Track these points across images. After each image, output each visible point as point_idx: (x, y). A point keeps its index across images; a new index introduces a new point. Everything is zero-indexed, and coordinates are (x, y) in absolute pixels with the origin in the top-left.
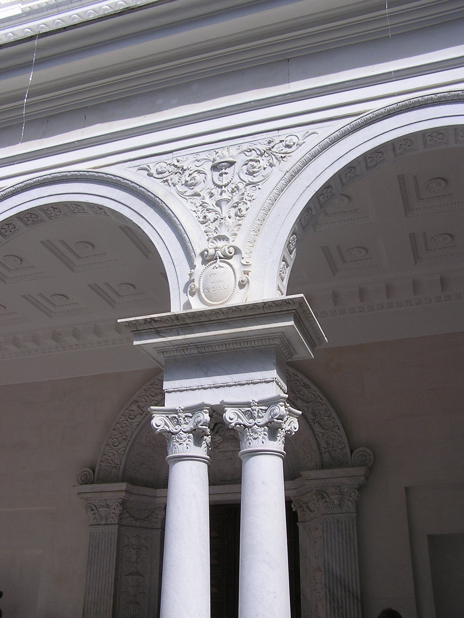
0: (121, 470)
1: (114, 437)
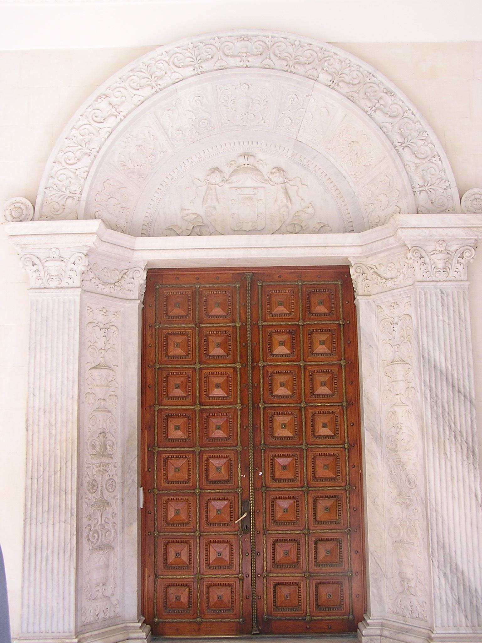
0: (83, 203)
1: (69, 149)
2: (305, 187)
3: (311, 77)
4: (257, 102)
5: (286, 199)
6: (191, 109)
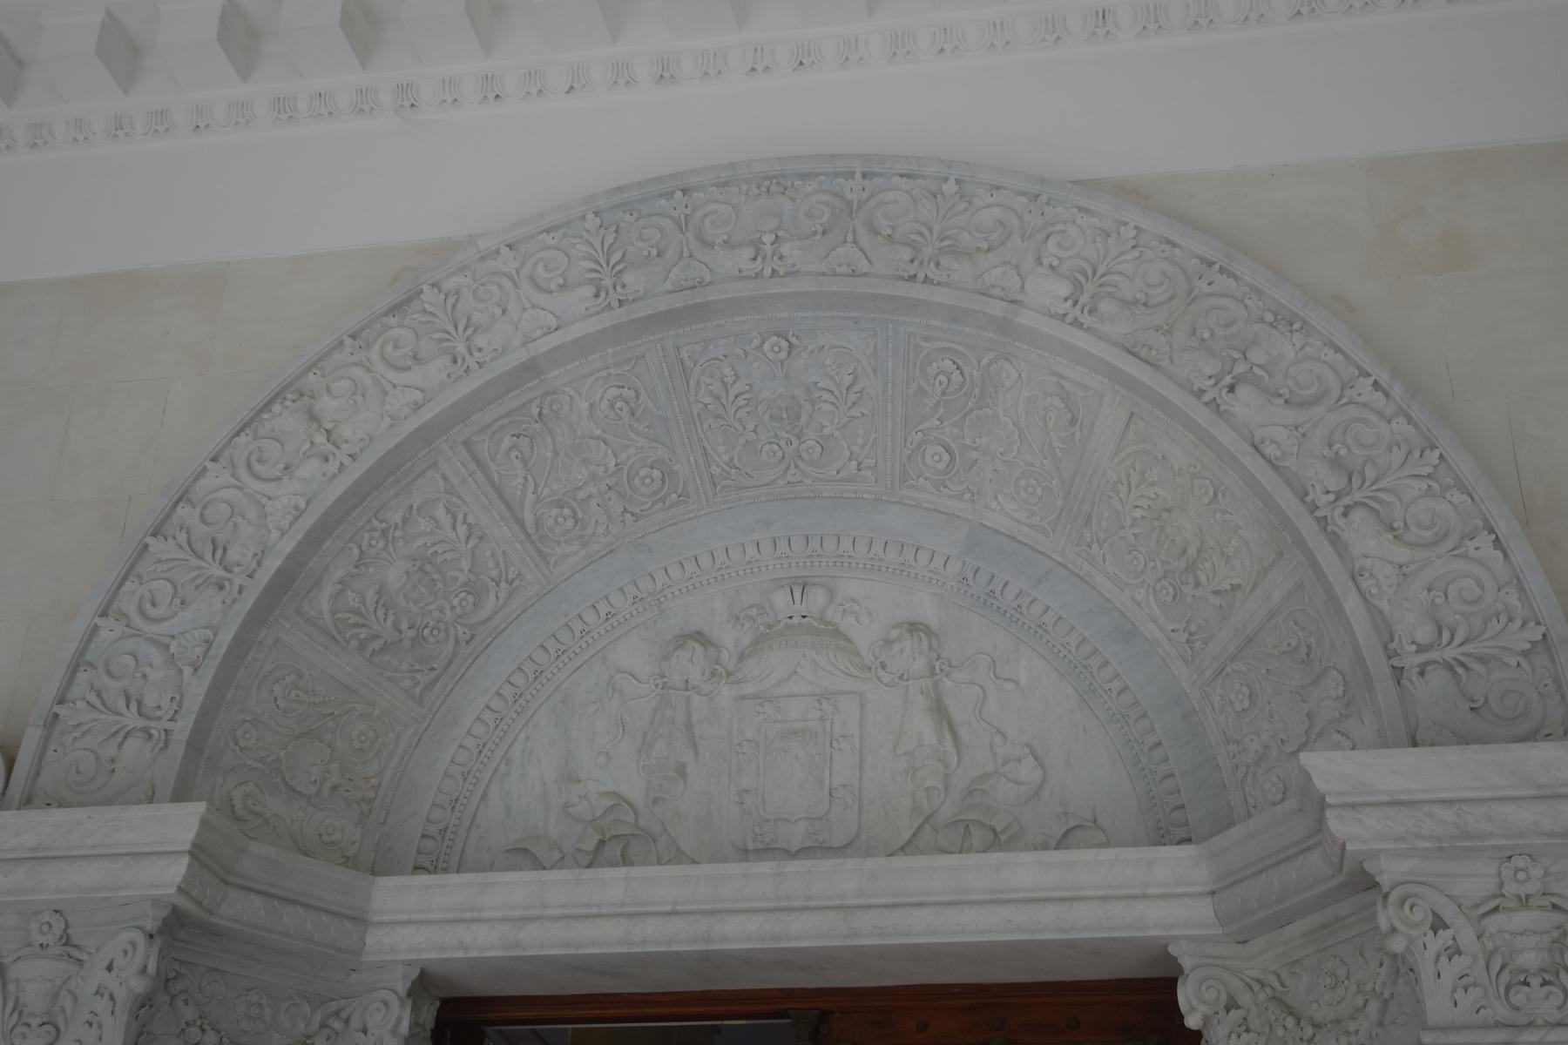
2: (1009, 686)
3: (996, 292)
4: (826, 396)
6: (598, 432)
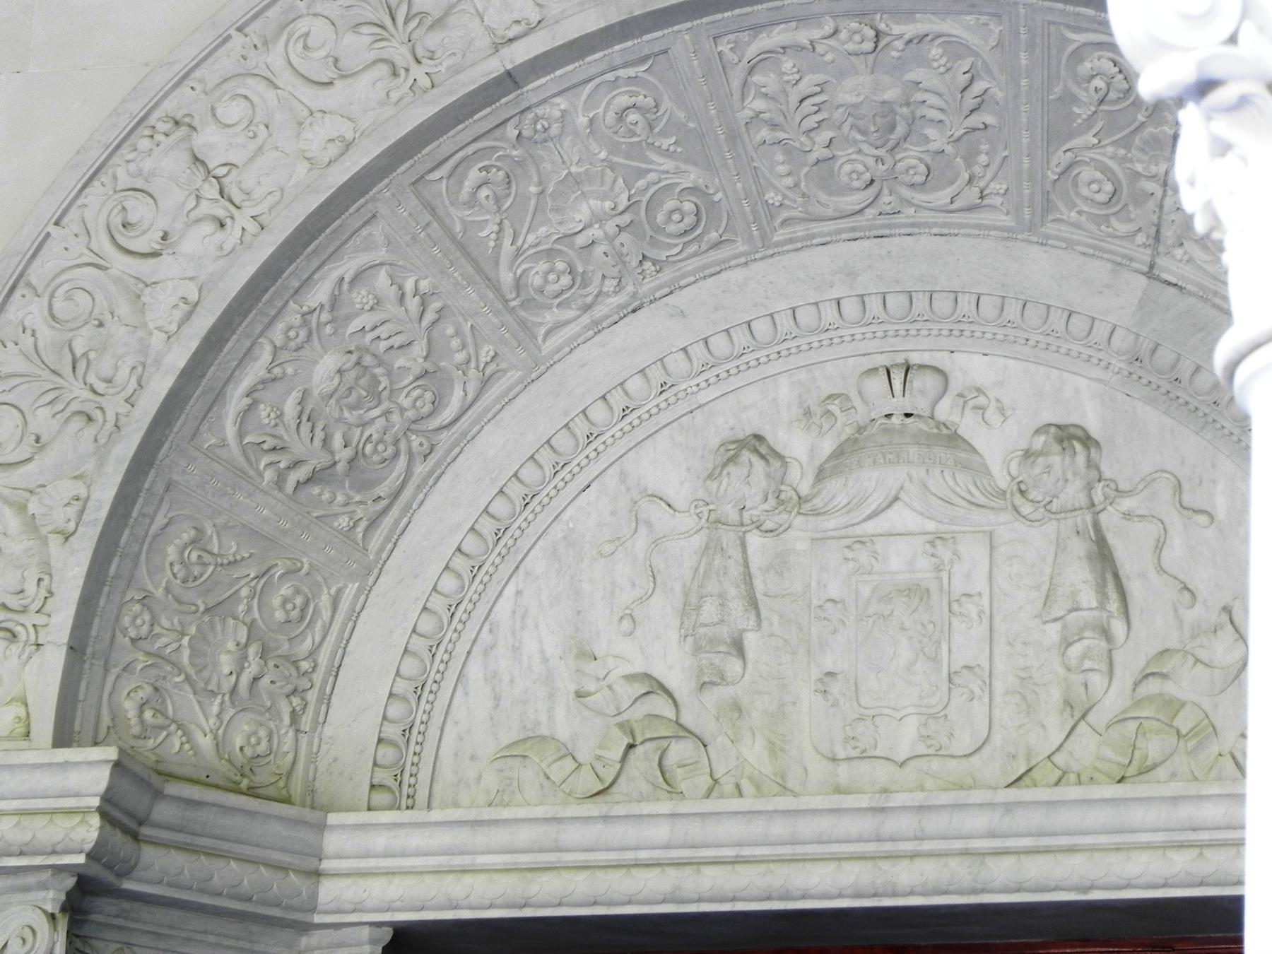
4: (932, 99)
5: (1101, 588)
